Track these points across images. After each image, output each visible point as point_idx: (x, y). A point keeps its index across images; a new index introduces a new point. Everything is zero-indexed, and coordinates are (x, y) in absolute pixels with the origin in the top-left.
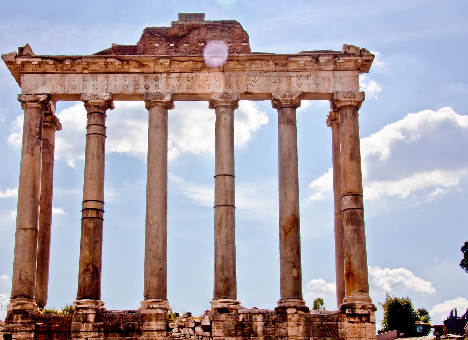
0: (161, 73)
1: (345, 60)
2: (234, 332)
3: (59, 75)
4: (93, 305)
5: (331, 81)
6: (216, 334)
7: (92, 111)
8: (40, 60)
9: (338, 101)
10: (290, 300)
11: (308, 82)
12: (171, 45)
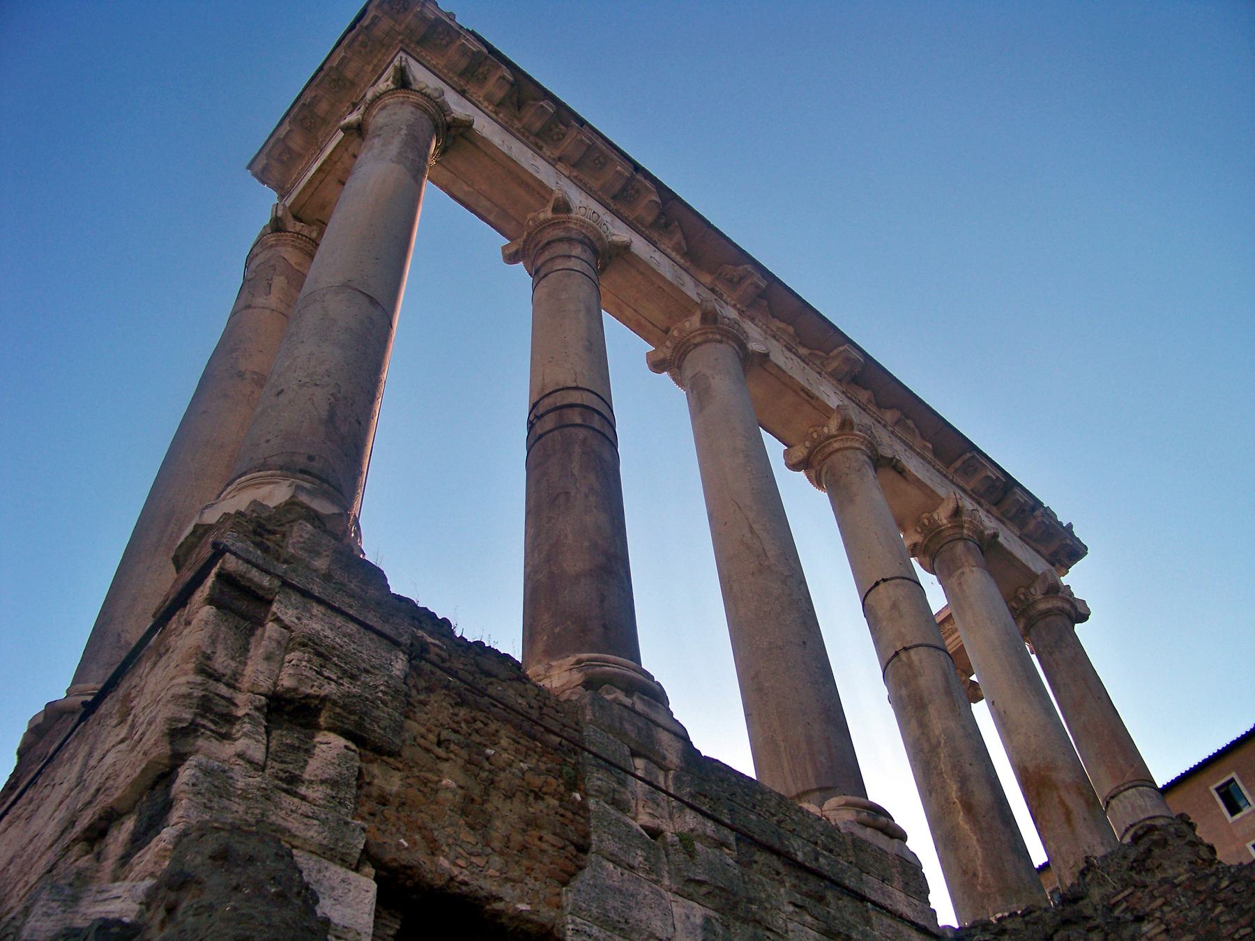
8: (485, 50)
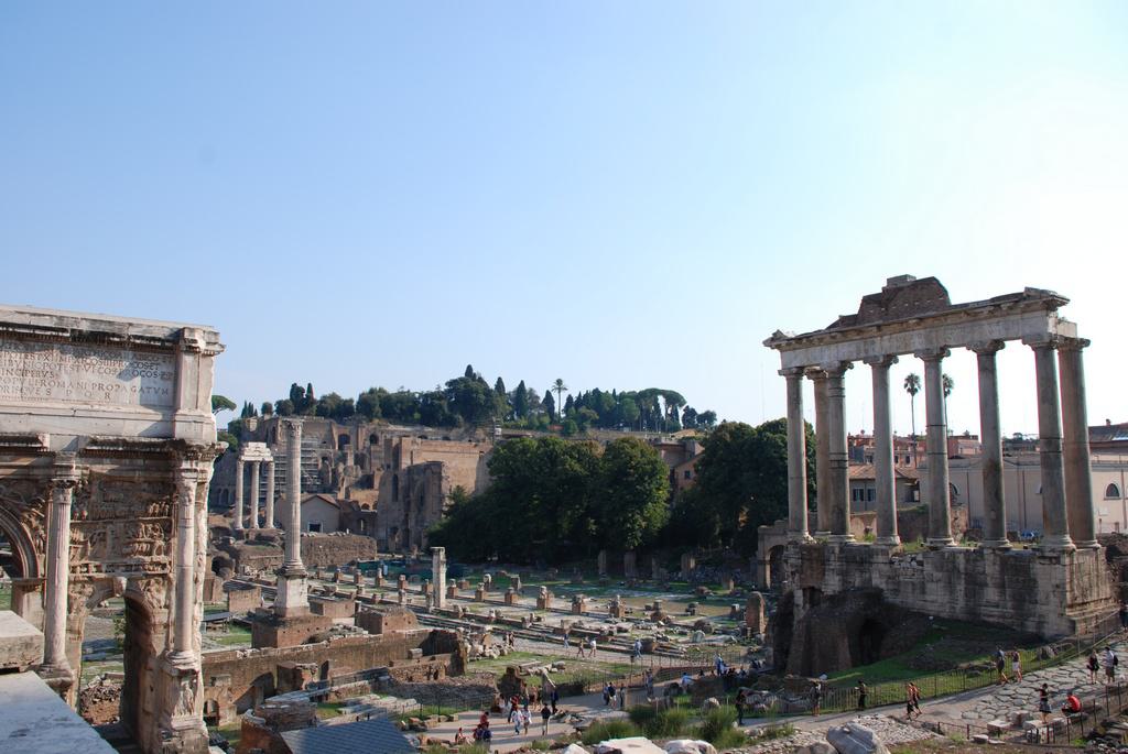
4: (838, 540)
11: (997, 328)
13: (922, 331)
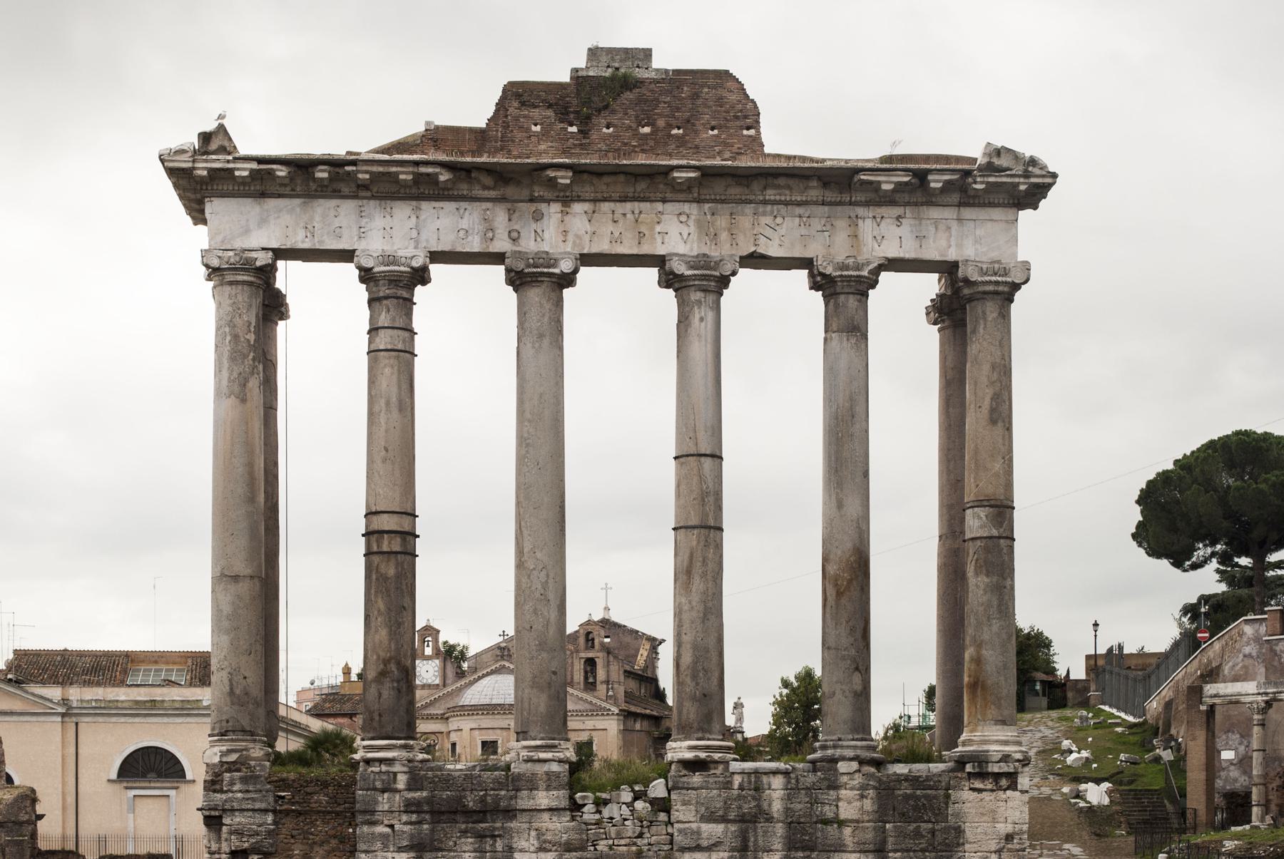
0: (549, 201)
1: (988, 183)
2: (721, 813)
3: (297, 201)
4: (404, 754)
5: (954, 232)
6: (682, 818)
7: (381, 294)
9: (967, 281)
10: (845, 743)
11: (899, 232)
12: (571, 129)
13: (691, 209)
